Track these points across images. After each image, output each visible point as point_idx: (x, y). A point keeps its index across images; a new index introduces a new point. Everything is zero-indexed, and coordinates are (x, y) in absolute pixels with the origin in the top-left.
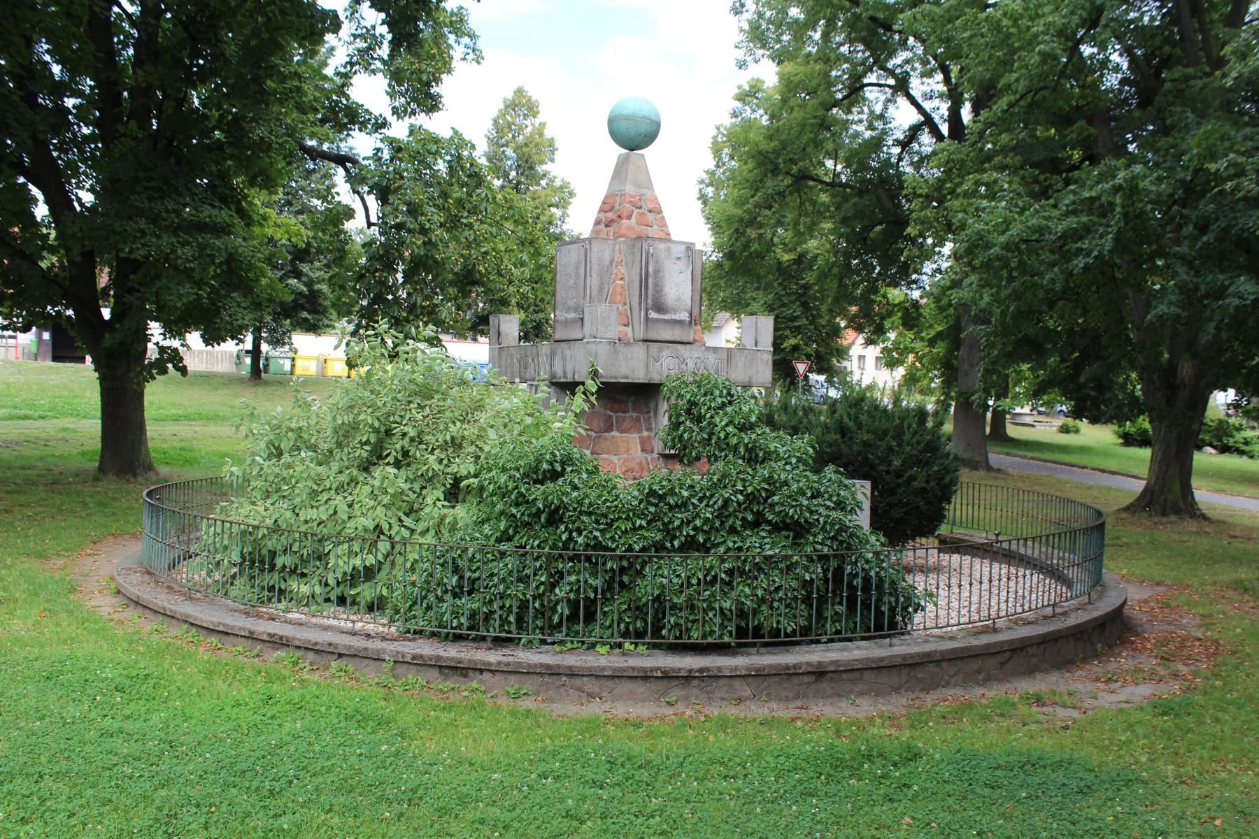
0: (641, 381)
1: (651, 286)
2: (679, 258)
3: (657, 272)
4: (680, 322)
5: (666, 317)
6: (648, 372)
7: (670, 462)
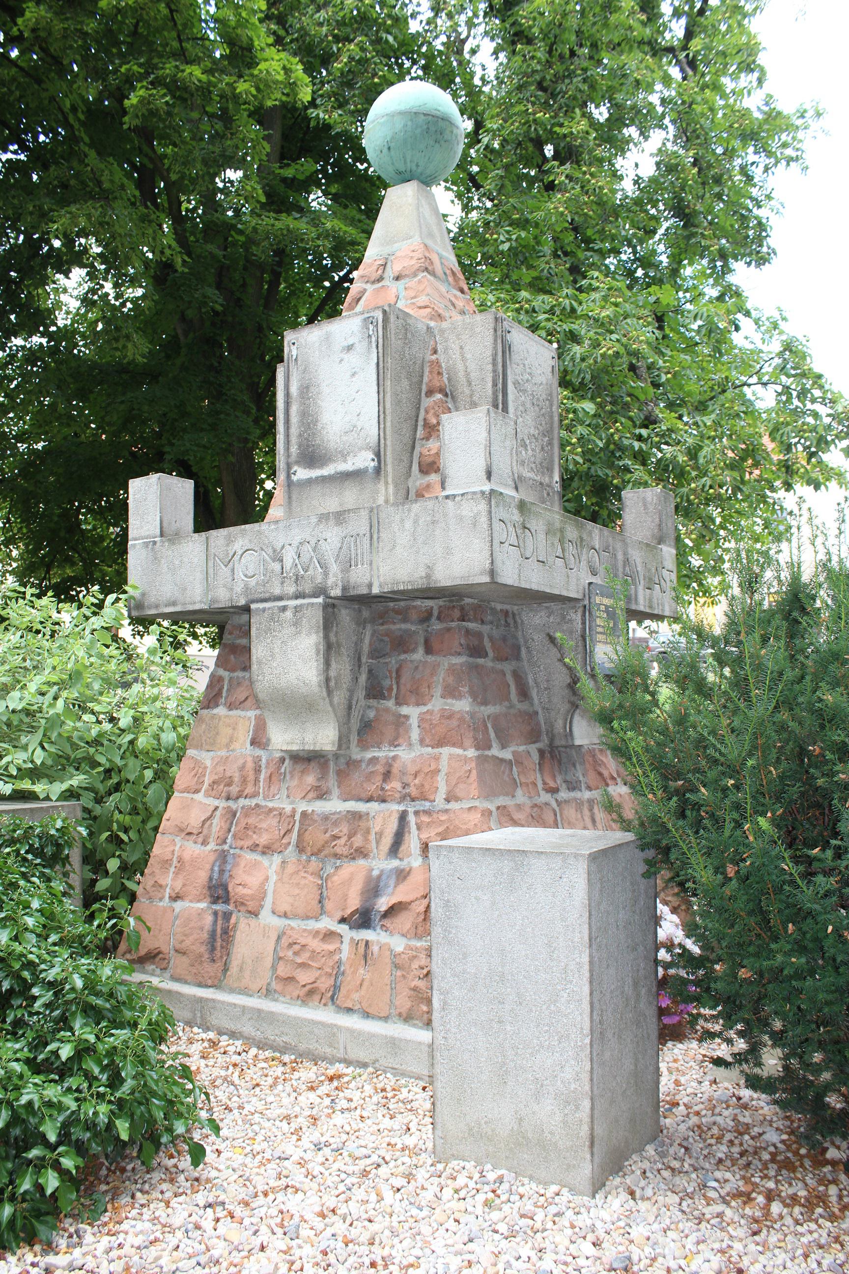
0: (197, 607)
1: (294, 419)
2: (350, 348)
3: (305, 390)
4: (355, 475)
5: (326, 471)
6: (208, 588)
7: (299, 767)
